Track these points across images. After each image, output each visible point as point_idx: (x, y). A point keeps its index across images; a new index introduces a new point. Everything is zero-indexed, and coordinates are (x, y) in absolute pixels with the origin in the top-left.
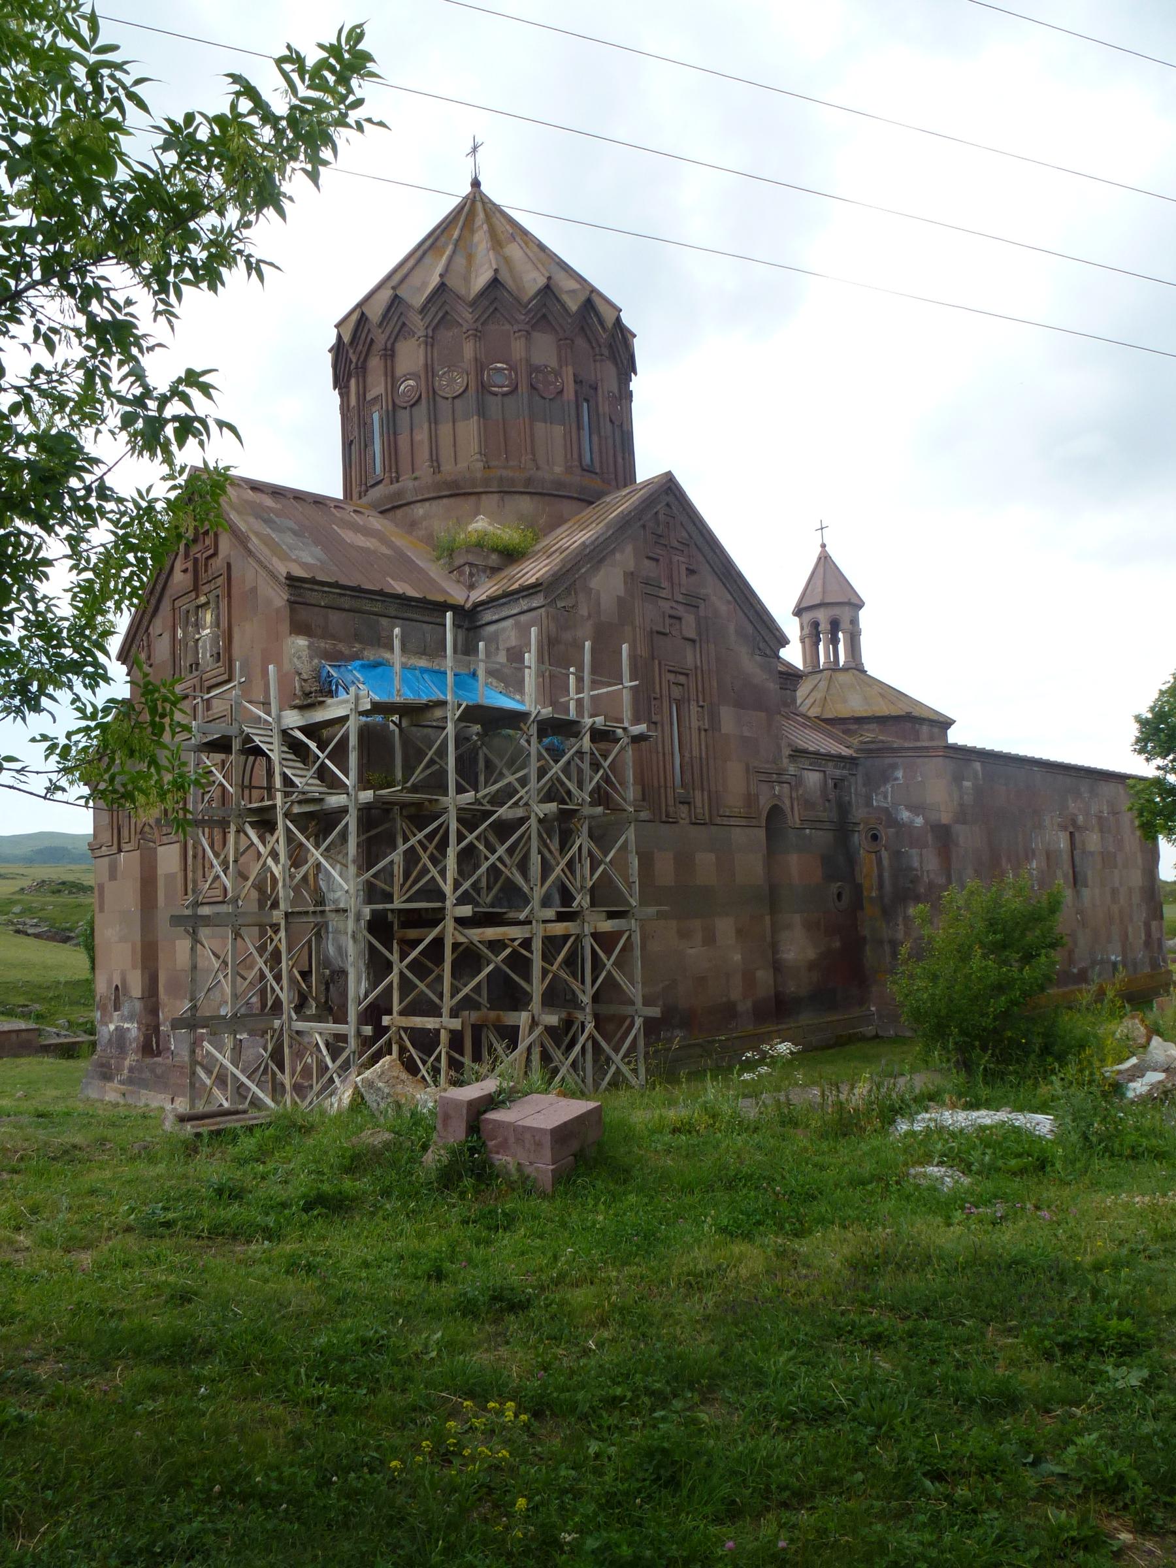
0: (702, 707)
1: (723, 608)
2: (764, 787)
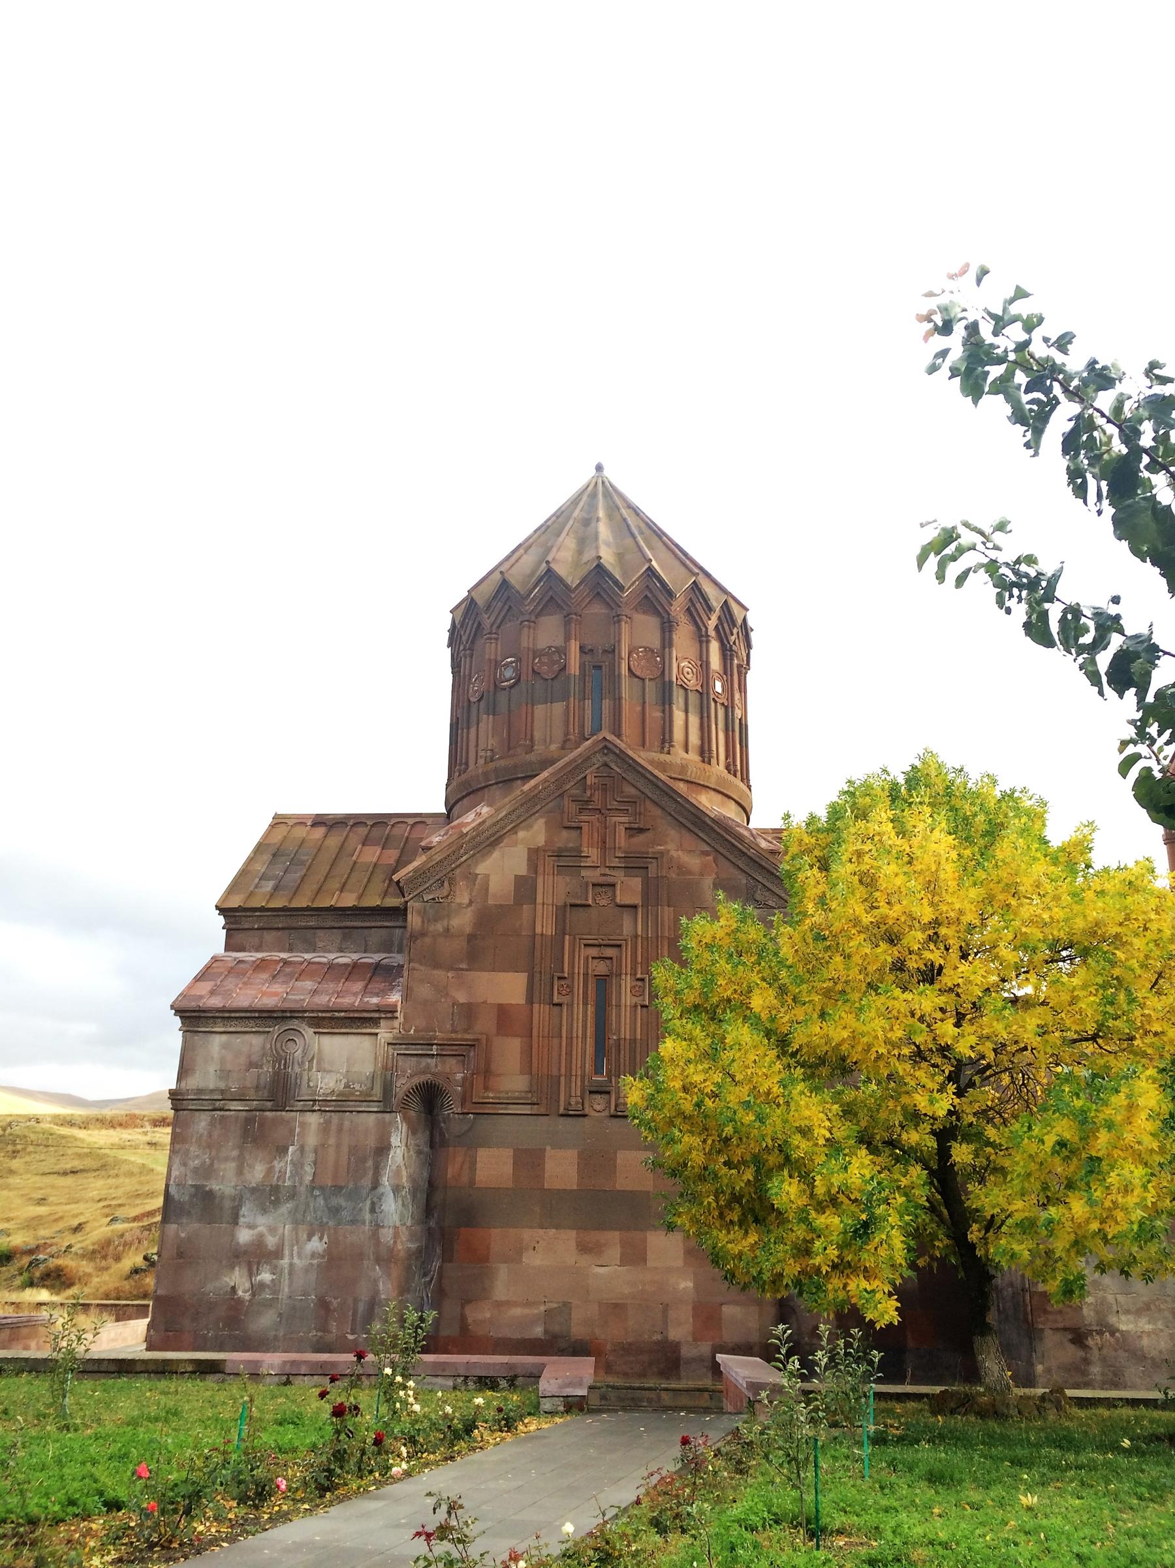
0: (642, 980)
1: (693, 862)
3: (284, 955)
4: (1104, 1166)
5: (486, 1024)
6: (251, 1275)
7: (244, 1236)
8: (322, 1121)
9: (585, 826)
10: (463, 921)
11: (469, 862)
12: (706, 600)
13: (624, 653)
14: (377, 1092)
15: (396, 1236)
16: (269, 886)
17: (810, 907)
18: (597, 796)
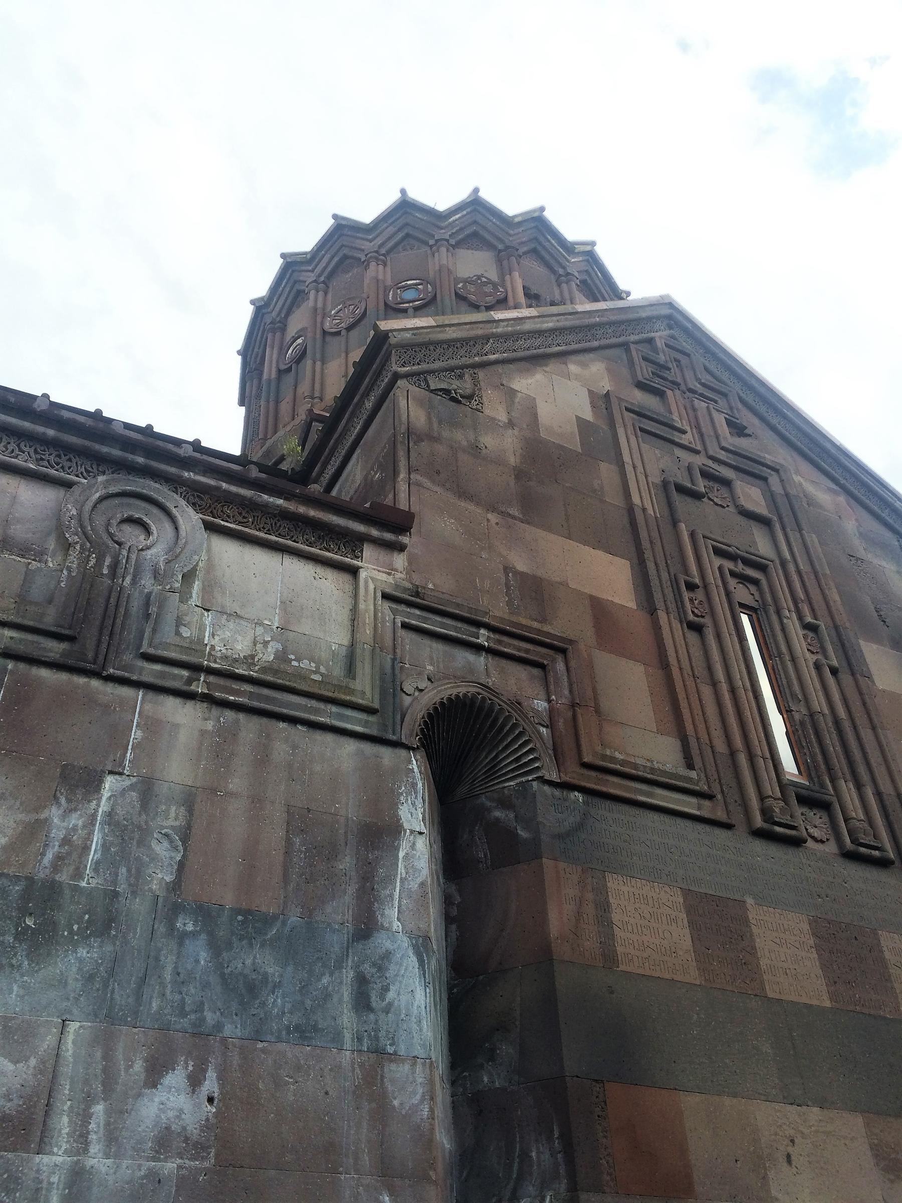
8: (210, 725)
11: (500, 368)
14: (364, 687)
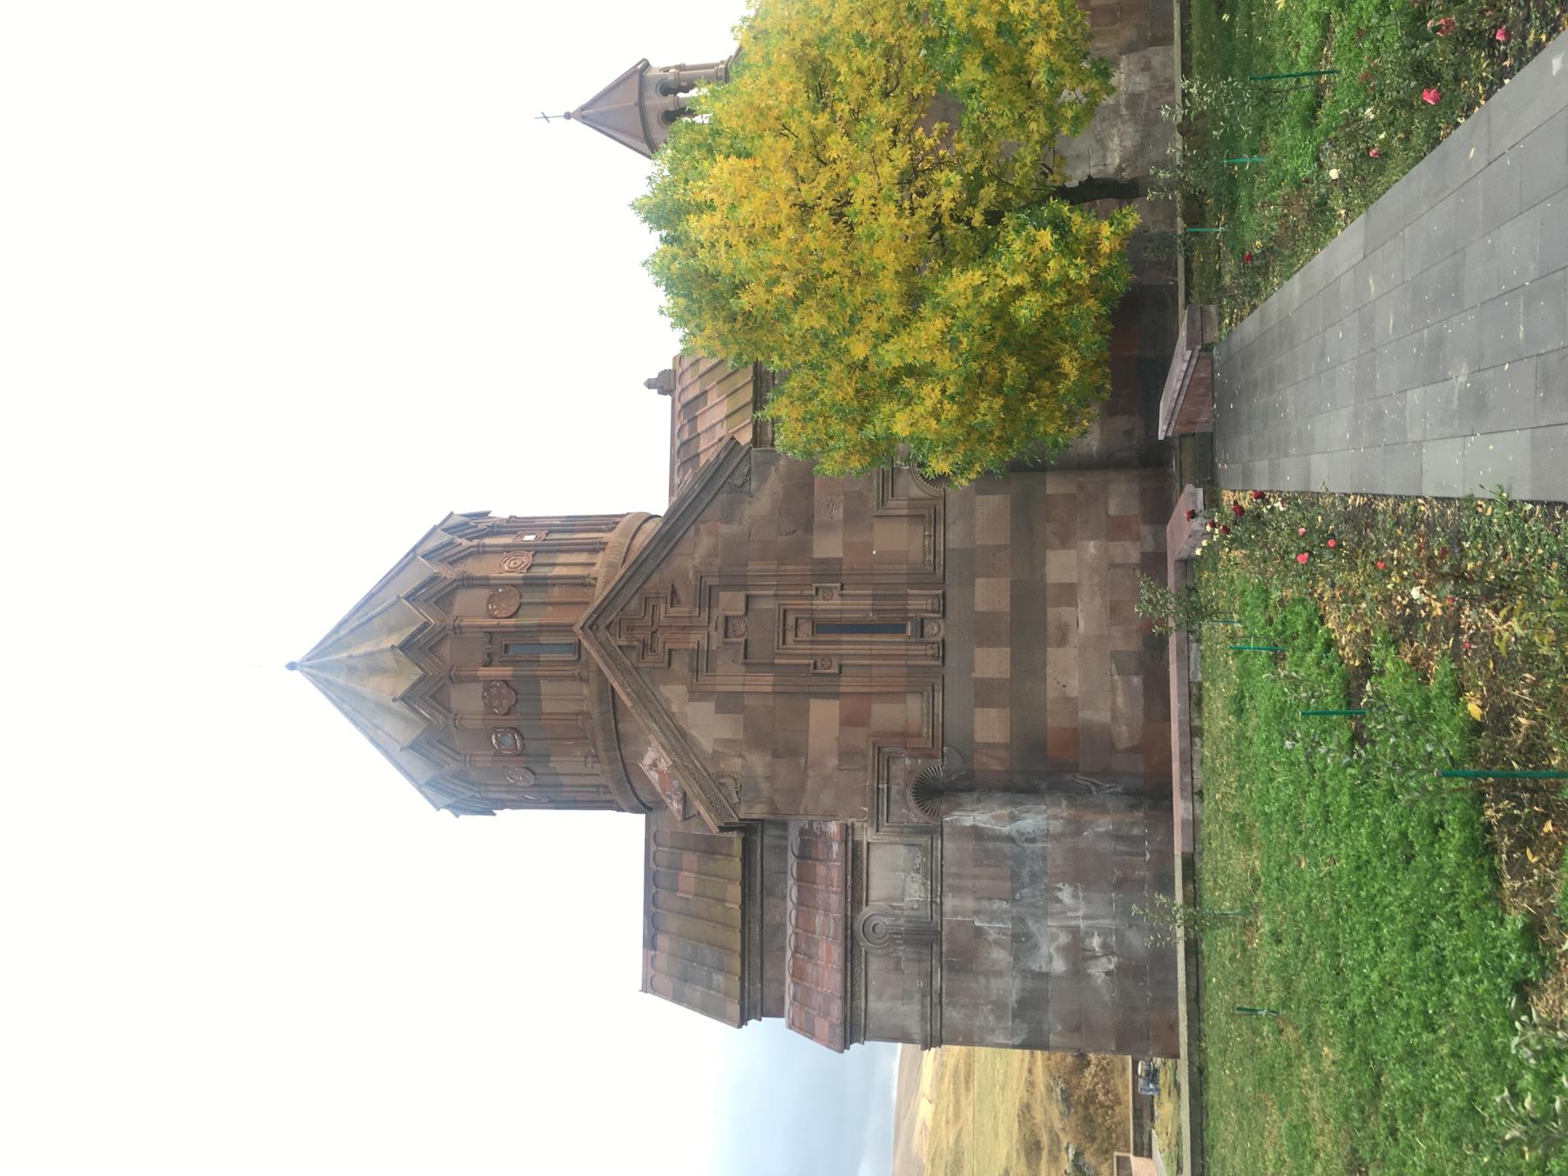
0: (817, 589)
1: (705, 543)
2: (901, 482)
3: (789, 954)
4: (1004, 20)
5: (859, 738)
6: (1095, 957)
7: (1059, 966)
9: (668, 646)
10: (759, 763)
12: (442, 546)
13: (494, 622)
14: (924, 840)
15: (1055, 817)
16: (718, 978)
17: (777, 290)
18: (640, 635)
